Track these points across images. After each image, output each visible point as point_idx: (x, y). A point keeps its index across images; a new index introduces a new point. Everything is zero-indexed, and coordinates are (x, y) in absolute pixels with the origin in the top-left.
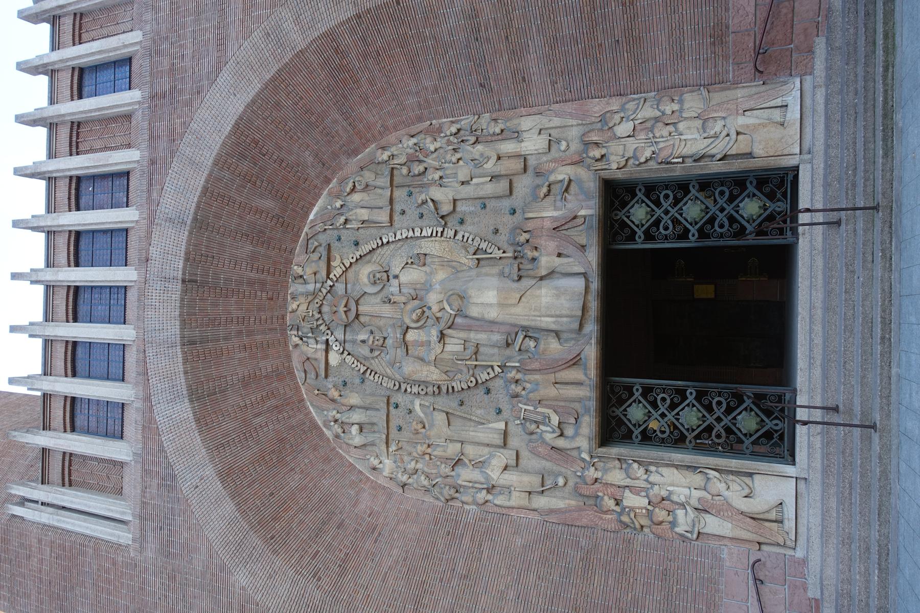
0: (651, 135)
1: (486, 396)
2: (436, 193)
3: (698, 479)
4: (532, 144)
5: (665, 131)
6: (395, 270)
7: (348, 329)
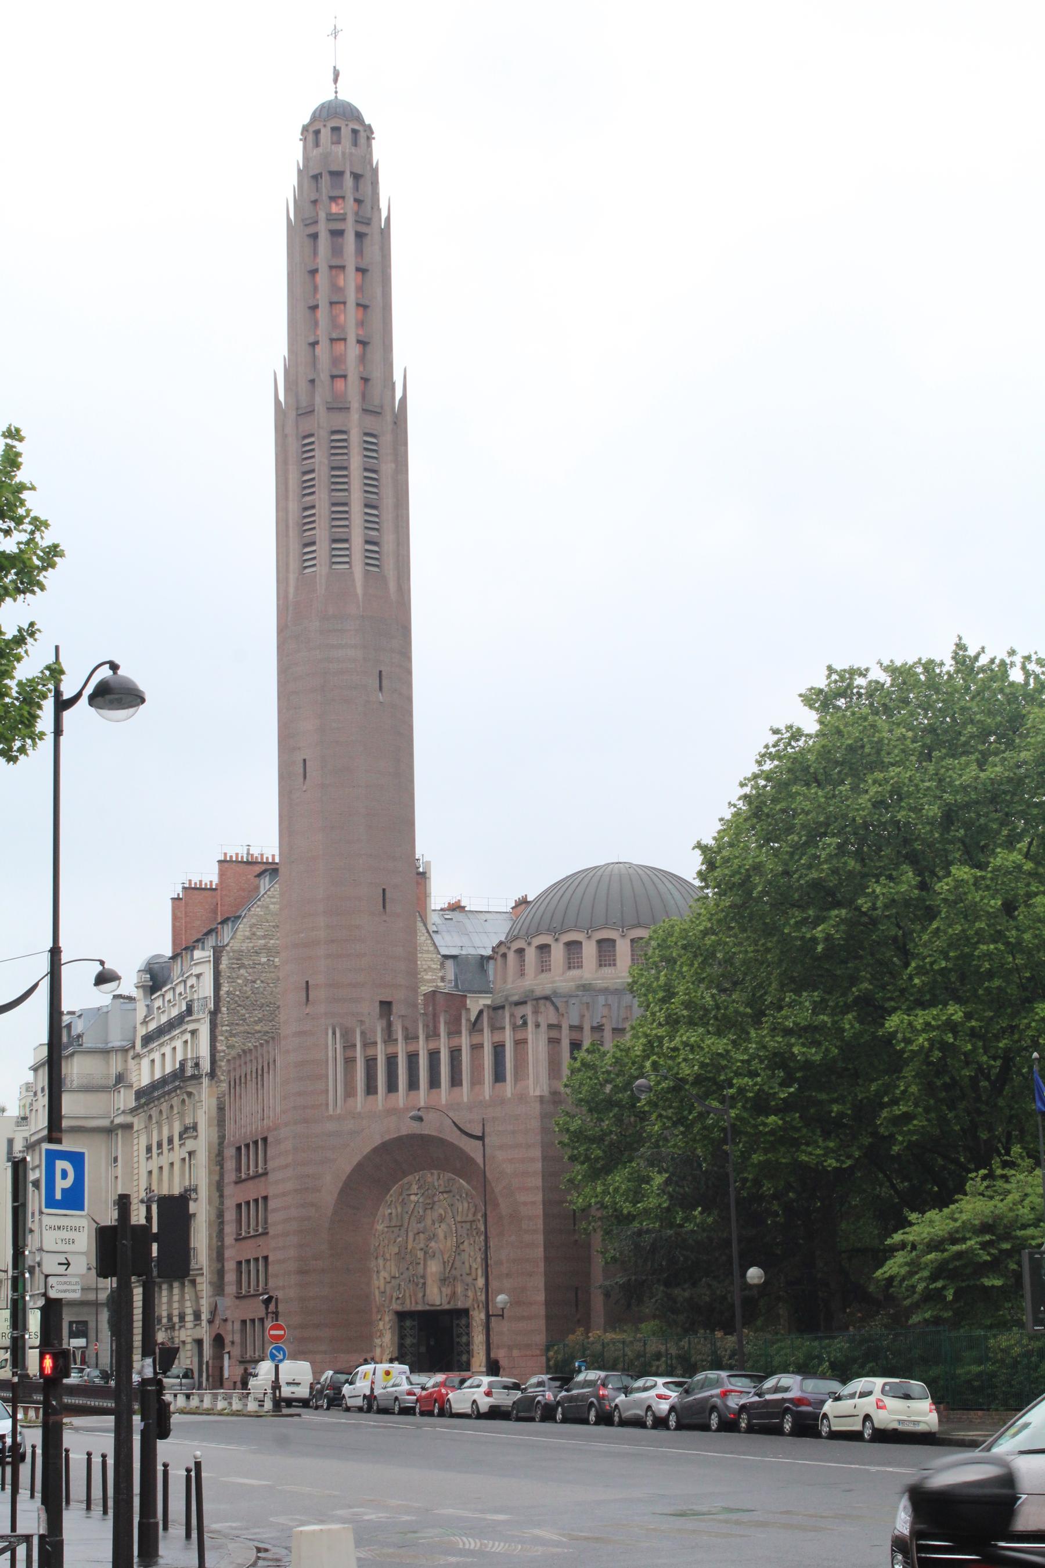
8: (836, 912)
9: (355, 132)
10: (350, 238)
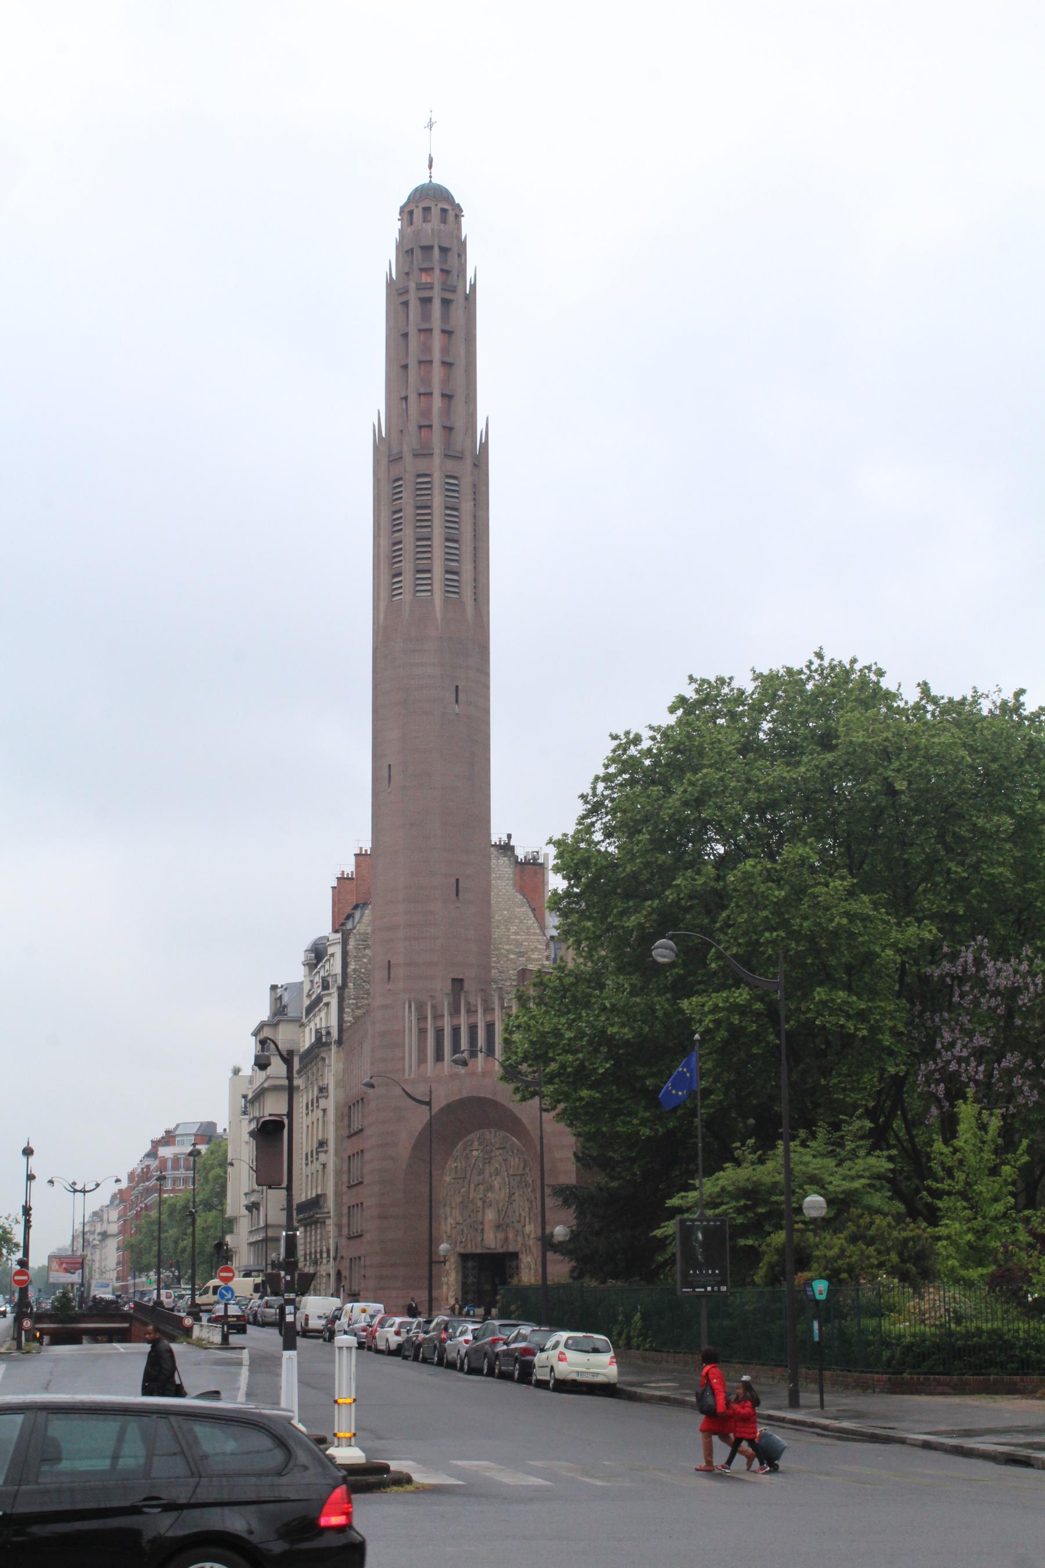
2: (517, 1194)
8: (649, 902)
9: (444, 211)
10: (437, 304)
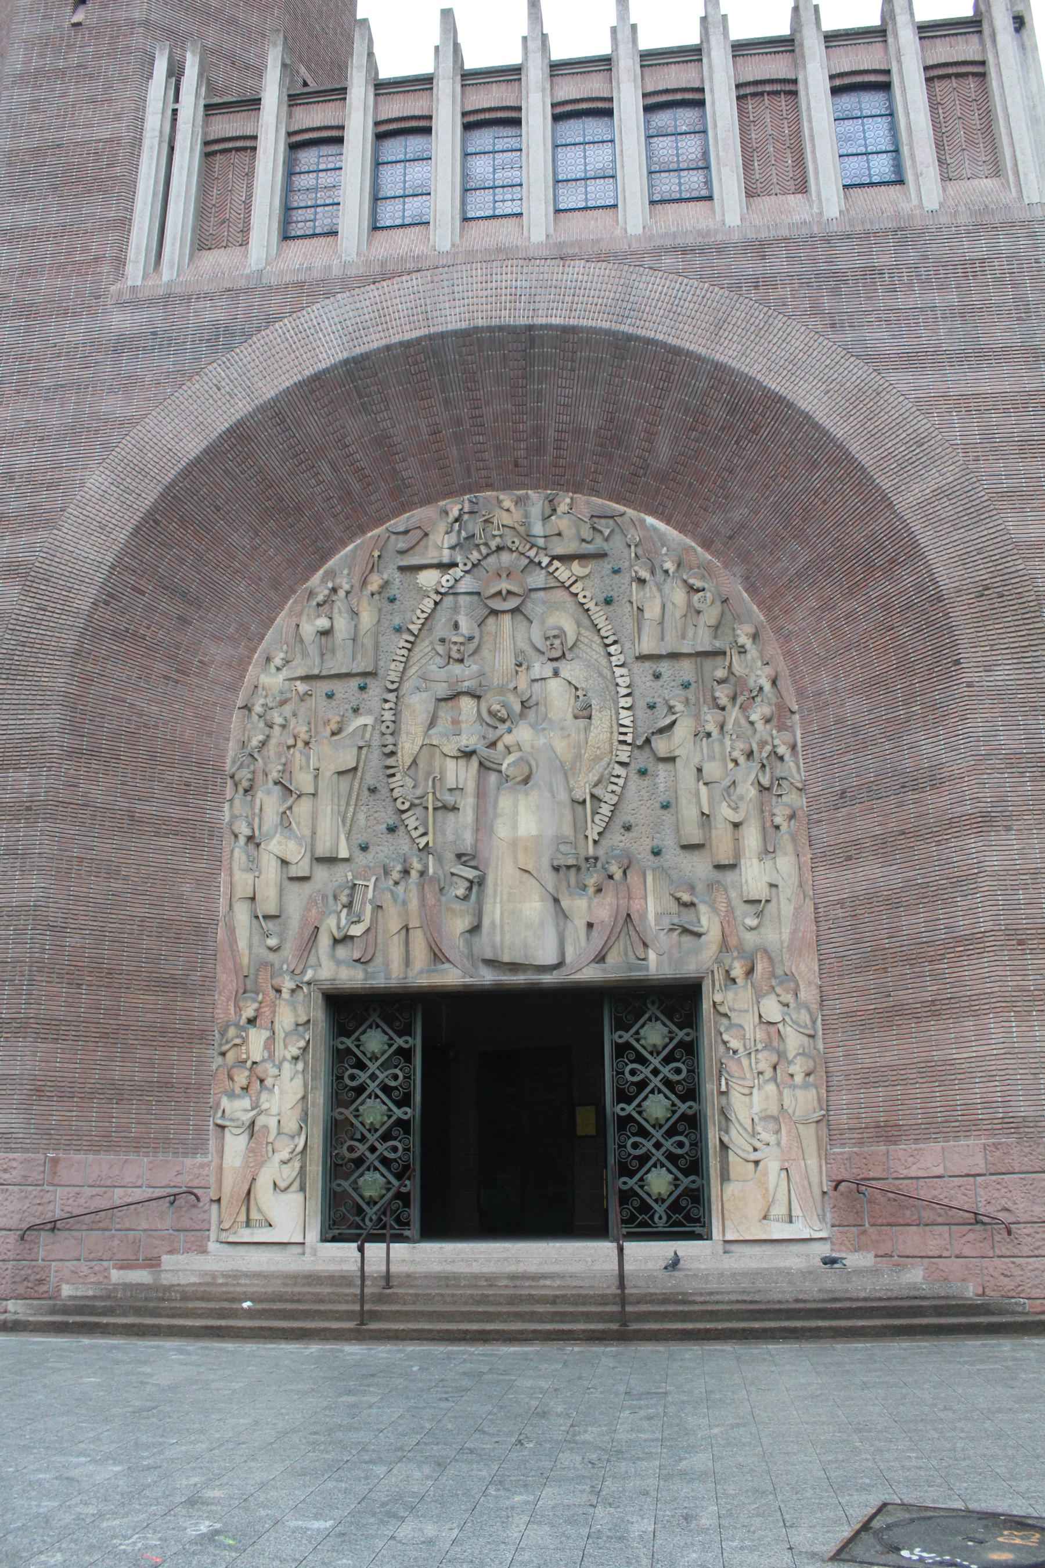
0: (759, 1047)
1: (384, 826)
2: (683, 731)
3: (291, 1124)
4: (754, 876)
5: (764, 1066)
6: (567, 670)
7: (476, 598)
